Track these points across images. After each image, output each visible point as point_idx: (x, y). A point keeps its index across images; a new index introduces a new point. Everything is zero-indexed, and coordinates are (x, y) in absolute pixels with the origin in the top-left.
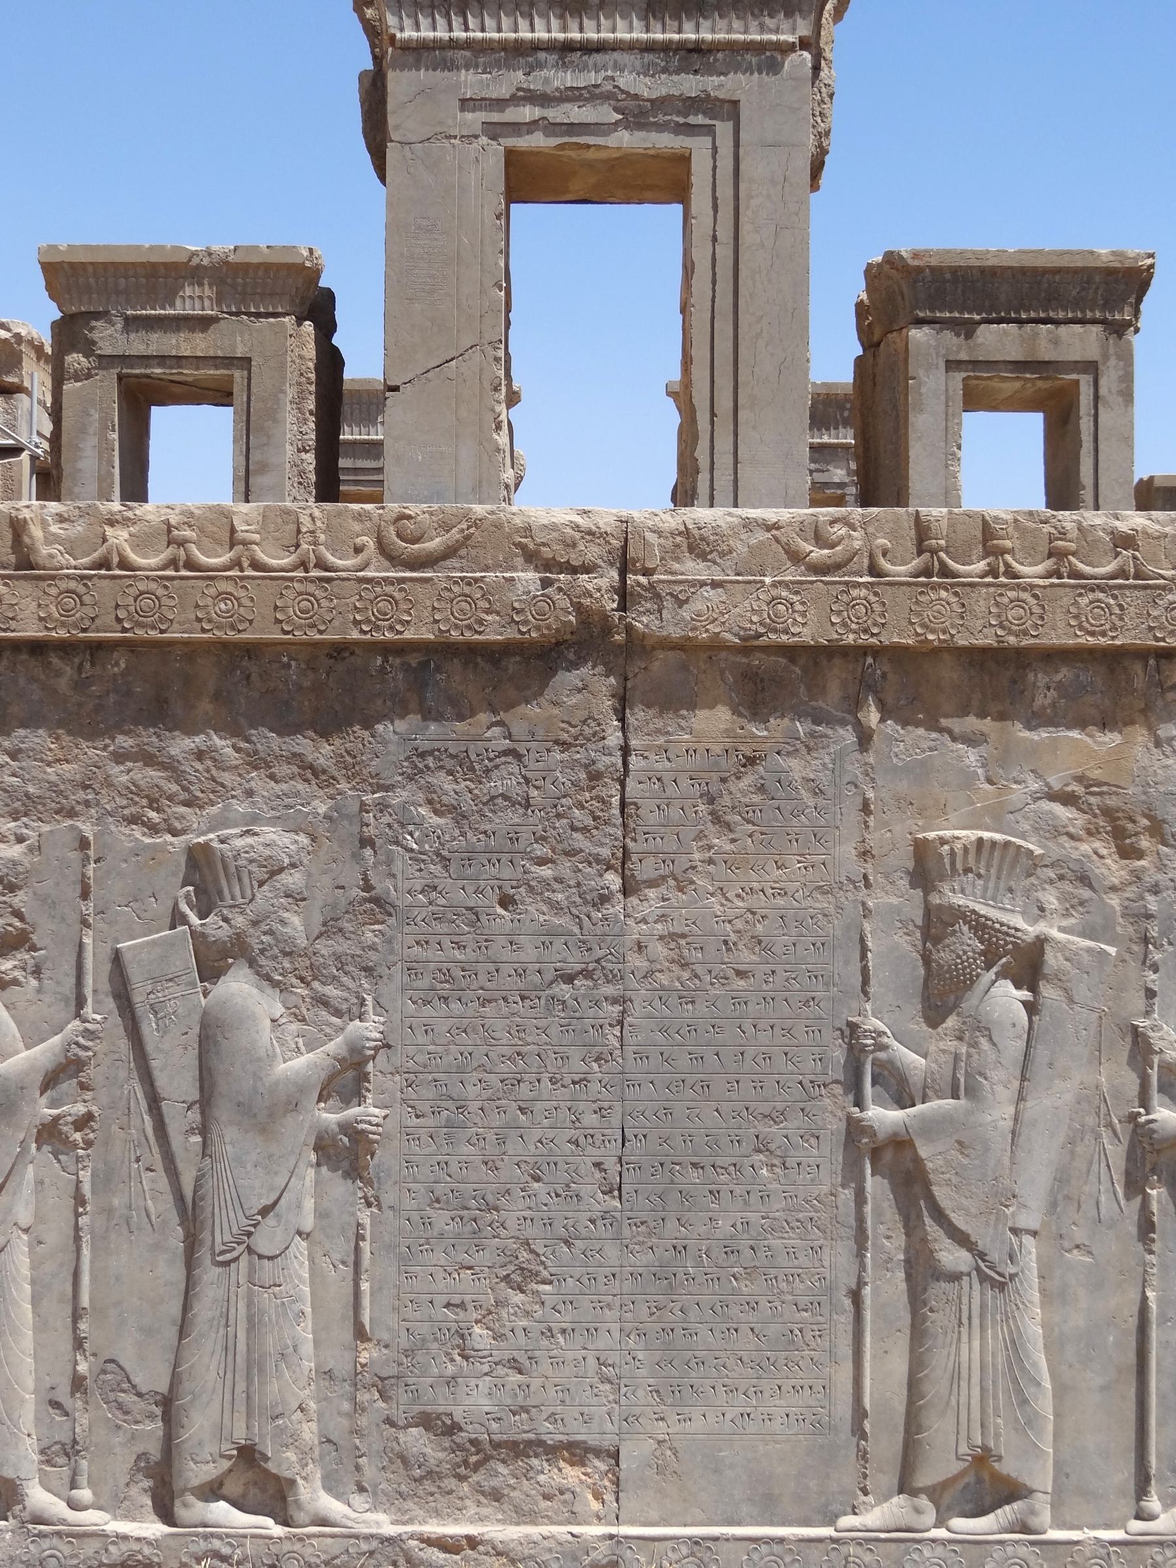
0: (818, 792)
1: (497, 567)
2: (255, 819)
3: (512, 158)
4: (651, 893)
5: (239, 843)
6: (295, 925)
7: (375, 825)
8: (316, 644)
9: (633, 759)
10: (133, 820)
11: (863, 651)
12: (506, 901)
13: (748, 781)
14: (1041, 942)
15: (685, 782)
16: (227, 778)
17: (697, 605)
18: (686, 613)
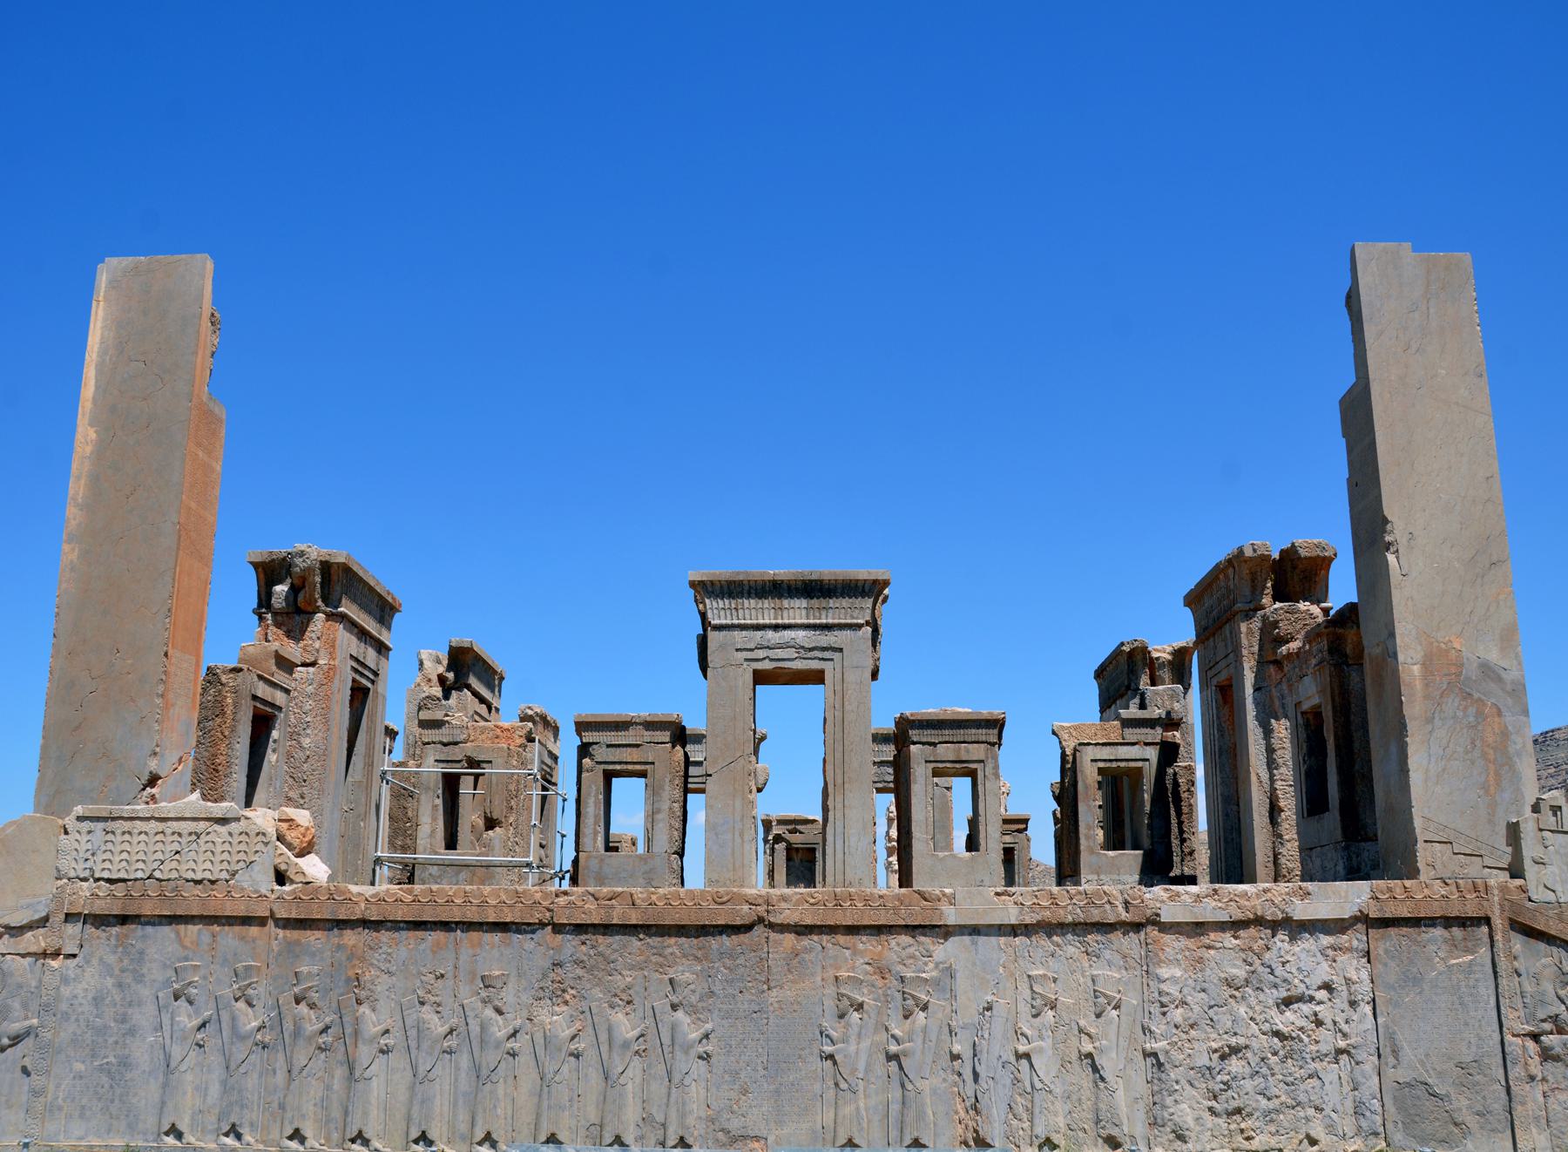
0: (812, 963)
1: (739, 905)
2: (684, 971)
3: (755, 672)
6: (694, 999)
7: (712, 972)
8: (698, 925)
11: (822, 926)
12: (741, 992)
14: (863, 1002)
16: (678, 960)
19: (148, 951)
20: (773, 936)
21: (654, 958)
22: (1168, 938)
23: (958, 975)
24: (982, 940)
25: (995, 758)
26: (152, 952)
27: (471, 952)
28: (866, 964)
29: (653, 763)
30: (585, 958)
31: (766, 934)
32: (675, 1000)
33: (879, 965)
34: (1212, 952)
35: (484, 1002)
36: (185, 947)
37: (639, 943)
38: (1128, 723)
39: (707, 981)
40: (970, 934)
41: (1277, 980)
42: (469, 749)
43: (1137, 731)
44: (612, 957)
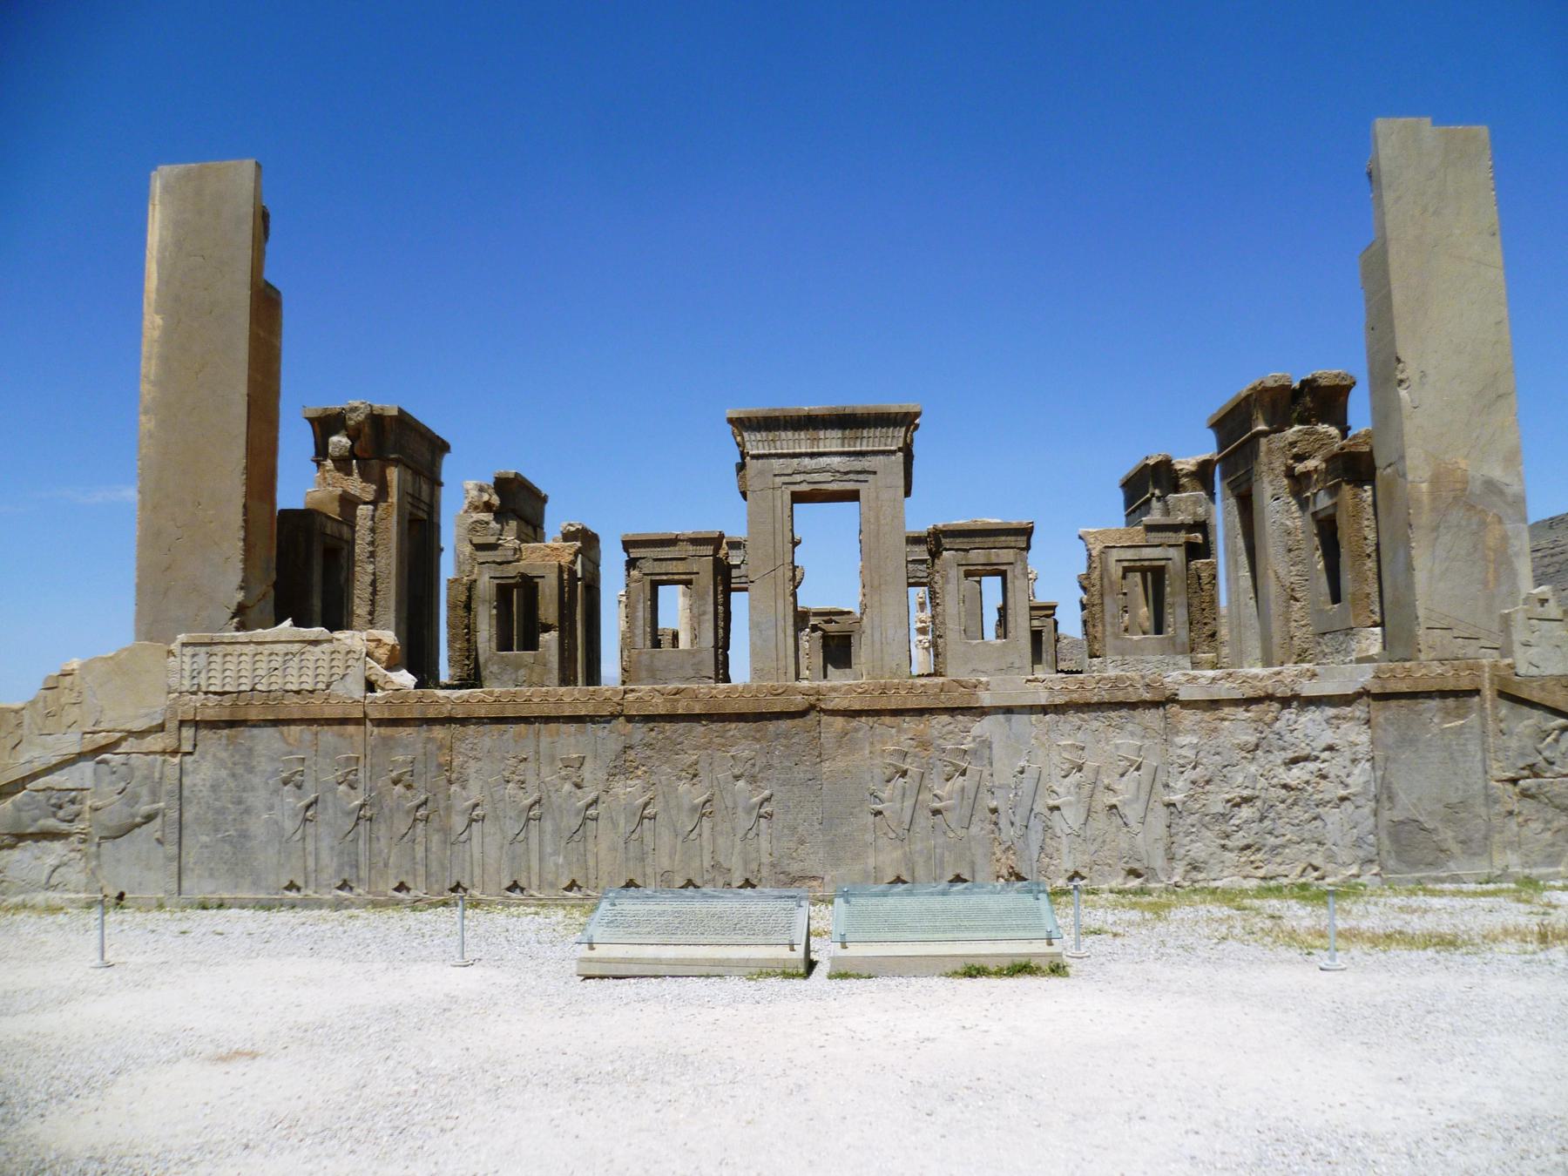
18: (832, 704)
19: (256, 748)
20: (825, 718)
21: (718, 740)
22: (1185, 712)
24: (1015, 717)
25: (1024, 560)
26: (260, 748)
27: (549, 740)
29: (698, 573)
30: (654, 742)
34: (1226, 723)
36: (289, 744)
37: (703, 728)
38: (1150, 528)
40: (1004, 713)
41: (1286, 744)
42: (522, 566)
43: (1160, 535)
44: (679, 740)
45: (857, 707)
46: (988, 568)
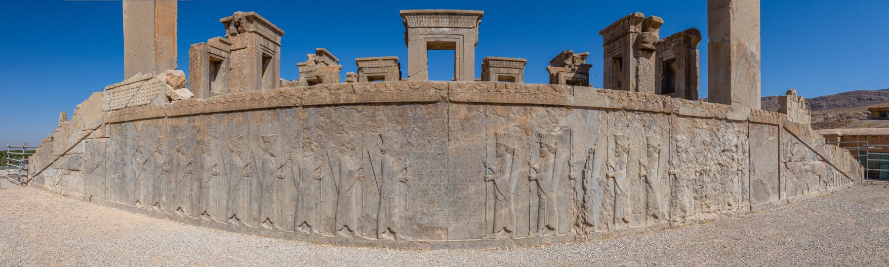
0: (479, 125)
2: (389, 130)
4: (453, 141)
5: (387, 134)
9: (449, 120)
10: (370, 130)
12: (429, 142)
13: (468, 124)
15: (458, 124)
16: (385, 124)
17: (460, 95)
20: (453, 107)
21: (369, 123)
23: (574, 134)
28: (516, 126)
30: (324, 125)
31: (447, 108)
32: (384, 148)
33: (525, 127)
35: (264, 150)
39: (405, 136)
44: (341, 123)
45: (477, 100)
46: (508, 75)
